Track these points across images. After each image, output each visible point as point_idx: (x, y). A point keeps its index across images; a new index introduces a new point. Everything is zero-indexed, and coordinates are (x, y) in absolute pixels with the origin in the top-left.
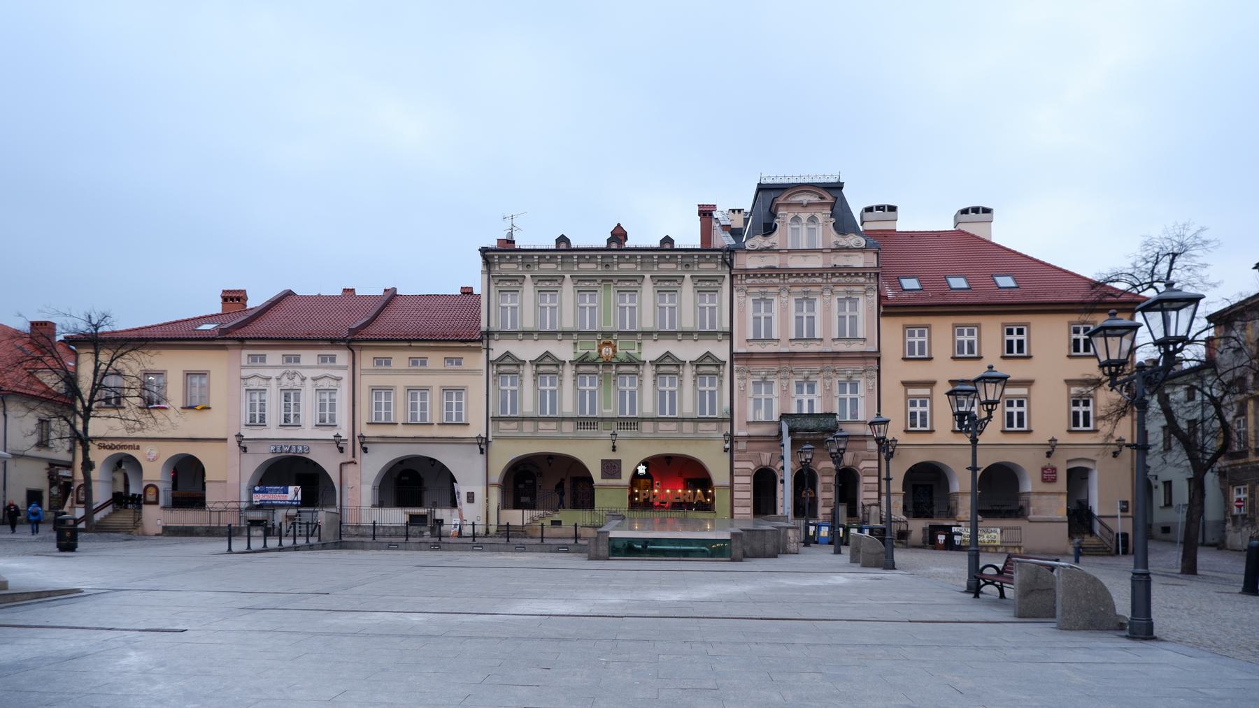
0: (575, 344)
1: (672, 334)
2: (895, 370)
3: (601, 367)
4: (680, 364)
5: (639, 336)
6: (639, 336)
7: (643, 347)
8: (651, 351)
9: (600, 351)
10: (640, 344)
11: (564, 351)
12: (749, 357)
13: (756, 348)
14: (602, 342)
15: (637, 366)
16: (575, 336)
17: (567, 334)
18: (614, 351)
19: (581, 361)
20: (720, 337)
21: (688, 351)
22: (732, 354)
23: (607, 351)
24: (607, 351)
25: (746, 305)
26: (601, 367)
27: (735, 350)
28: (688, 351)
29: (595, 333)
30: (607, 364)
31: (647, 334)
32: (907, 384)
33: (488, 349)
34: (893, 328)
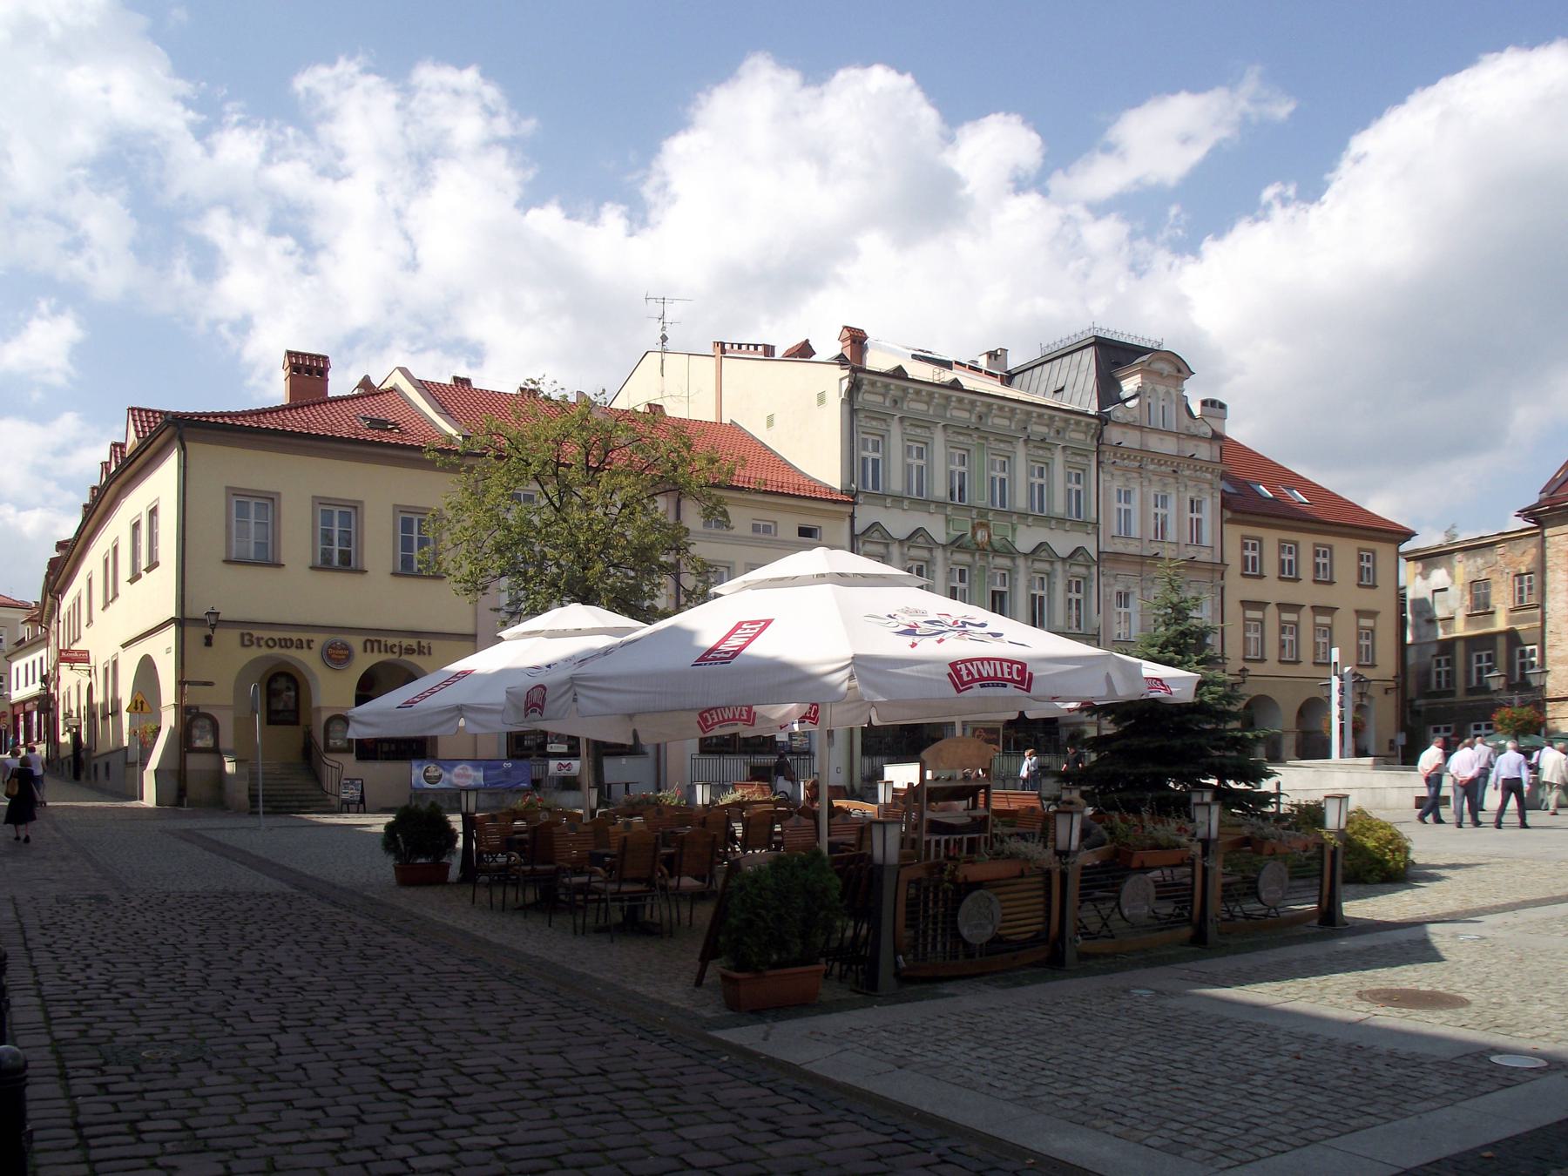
0: (948, 521)
1: (1046, 520)
2: (1239, 588)
3: (977, 557)
4: (1053, 557)
5: (1015, 517)
6: (1015, 517)
7: (1018, 533)
8: (1026, 539)
9: (974, 535)
10: (1014, 530)
11: (938, 529)
12: (1117, 557)
13: (1119, 547)
14: (976, 521)
15: (1013, 559)
16: (949, 510)
17: (941, 504)
18: (989, 536)
19: (957, 544)
20: (1090, 527)
21: (1063, 543)
22: (1099, 552)
23: (981, 535)
24: (981, 535)
25: (1113, 484)
26: (977, 557)
27: (1101, 550)
28: (1063, 543)
29: (970, 508)
30: (982, 549)
31: (1023, 516)
32: (1246, 604)
33: (852, 517)
34: (1234, 533)
